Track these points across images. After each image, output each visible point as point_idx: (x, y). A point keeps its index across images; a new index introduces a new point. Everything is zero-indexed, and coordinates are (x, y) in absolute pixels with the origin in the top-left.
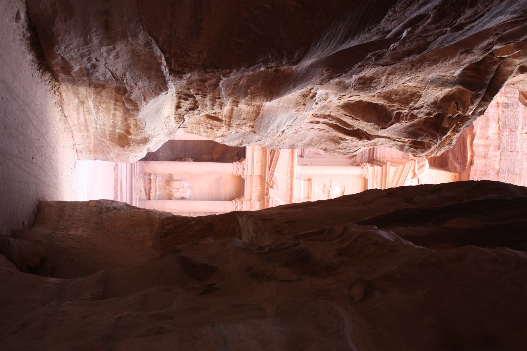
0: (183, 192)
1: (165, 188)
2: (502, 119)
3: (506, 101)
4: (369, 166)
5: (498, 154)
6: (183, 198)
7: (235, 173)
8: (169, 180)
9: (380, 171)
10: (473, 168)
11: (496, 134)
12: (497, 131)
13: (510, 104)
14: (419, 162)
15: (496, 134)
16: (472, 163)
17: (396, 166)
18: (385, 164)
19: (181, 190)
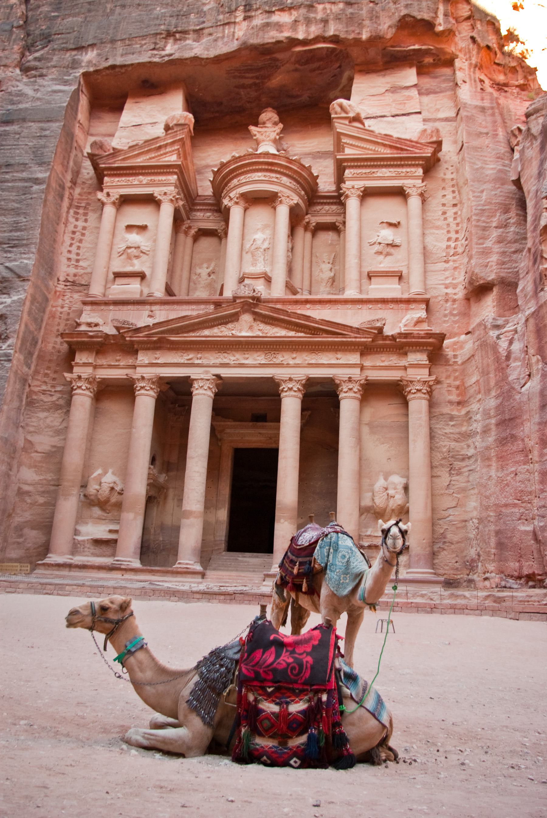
0: (395, 489)
2: (267, 8)
3: (242, 8)
5: (320, 7)
6: (406, 488)
7: (358, 396)
9: (352, 170)
10: (342, 36)
11: (291, 14)
12: (286, 13)
14: (336, 113)
16: (335, 39)
17: (344, 149)
19: (391, 492)
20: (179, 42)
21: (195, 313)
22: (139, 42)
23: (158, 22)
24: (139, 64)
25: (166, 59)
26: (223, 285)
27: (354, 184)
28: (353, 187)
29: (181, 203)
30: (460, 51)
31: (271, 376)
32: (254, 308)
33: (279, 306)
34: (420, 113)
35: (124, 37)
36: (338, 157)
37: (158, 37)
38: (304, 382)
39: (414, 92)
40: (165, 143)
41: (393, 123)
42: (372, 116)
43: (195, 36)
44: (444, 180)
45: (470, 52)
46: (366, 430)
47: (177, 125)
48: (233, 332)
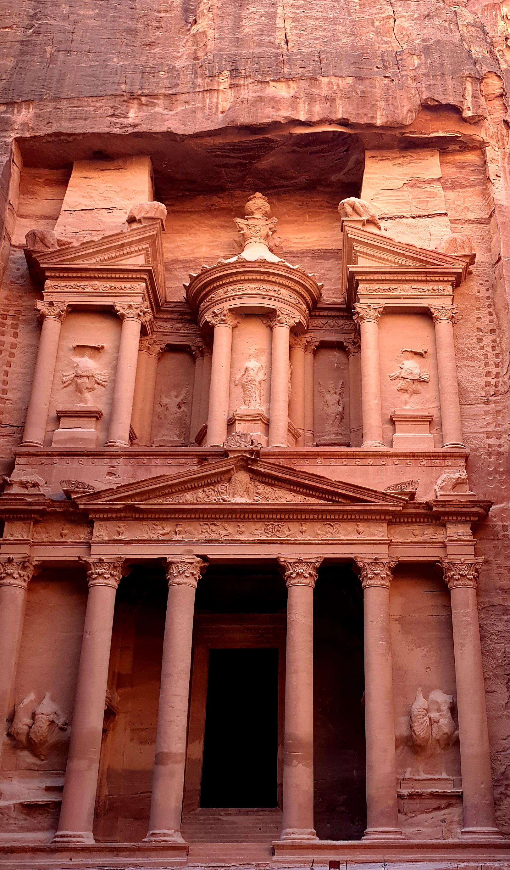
0: (439, 710)
1: (431, 756)
4: (359, 306)
8: (411, 745)
9: (367, 286)
13: (233, 67)
15: (289, 87)
17: (356, 257)
18: (352, 275)
19: (434, 715)
20: (145, 108)
21: (172, 471)
22: (92, 104)
23: (117, 79)
24: (93, 134)
25: (130, 130)
26: (206, 427)
27: (368, 302)
28: (369, 308)
29: (149, 317)
30: (492, 137)
31: (275, 556)
32: (252, 465)
33: (283, 461)
34: (446, 214)
35: (73, 95)
36: (350, 270)
37: (118, 99)
38: (317, 565)
39: (438, 188)
40: (130, 240)
41: (415, 226)
42: (388, 216)
43: (167, 102)
44: (478, 299)
45: (503, 139)
46: (396, 627)
47: (144, 218)
48: (225, 497)
